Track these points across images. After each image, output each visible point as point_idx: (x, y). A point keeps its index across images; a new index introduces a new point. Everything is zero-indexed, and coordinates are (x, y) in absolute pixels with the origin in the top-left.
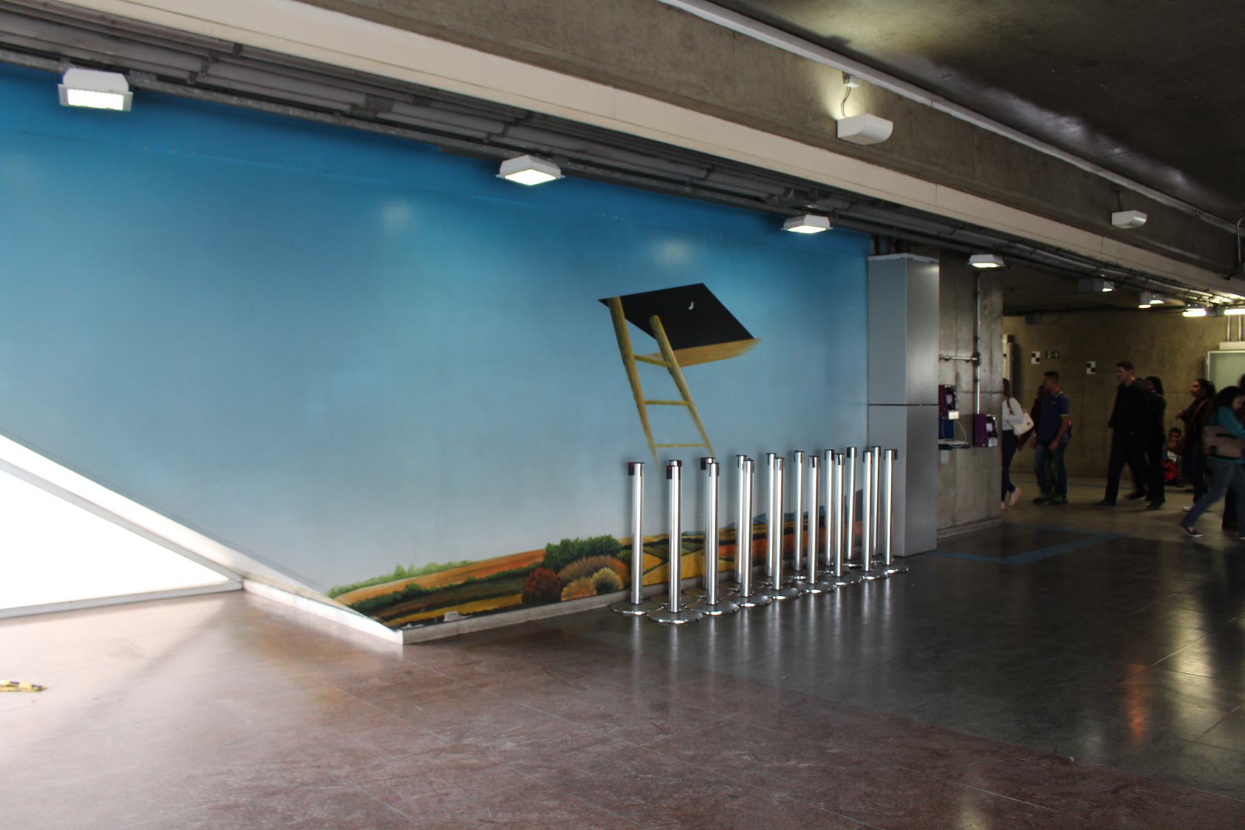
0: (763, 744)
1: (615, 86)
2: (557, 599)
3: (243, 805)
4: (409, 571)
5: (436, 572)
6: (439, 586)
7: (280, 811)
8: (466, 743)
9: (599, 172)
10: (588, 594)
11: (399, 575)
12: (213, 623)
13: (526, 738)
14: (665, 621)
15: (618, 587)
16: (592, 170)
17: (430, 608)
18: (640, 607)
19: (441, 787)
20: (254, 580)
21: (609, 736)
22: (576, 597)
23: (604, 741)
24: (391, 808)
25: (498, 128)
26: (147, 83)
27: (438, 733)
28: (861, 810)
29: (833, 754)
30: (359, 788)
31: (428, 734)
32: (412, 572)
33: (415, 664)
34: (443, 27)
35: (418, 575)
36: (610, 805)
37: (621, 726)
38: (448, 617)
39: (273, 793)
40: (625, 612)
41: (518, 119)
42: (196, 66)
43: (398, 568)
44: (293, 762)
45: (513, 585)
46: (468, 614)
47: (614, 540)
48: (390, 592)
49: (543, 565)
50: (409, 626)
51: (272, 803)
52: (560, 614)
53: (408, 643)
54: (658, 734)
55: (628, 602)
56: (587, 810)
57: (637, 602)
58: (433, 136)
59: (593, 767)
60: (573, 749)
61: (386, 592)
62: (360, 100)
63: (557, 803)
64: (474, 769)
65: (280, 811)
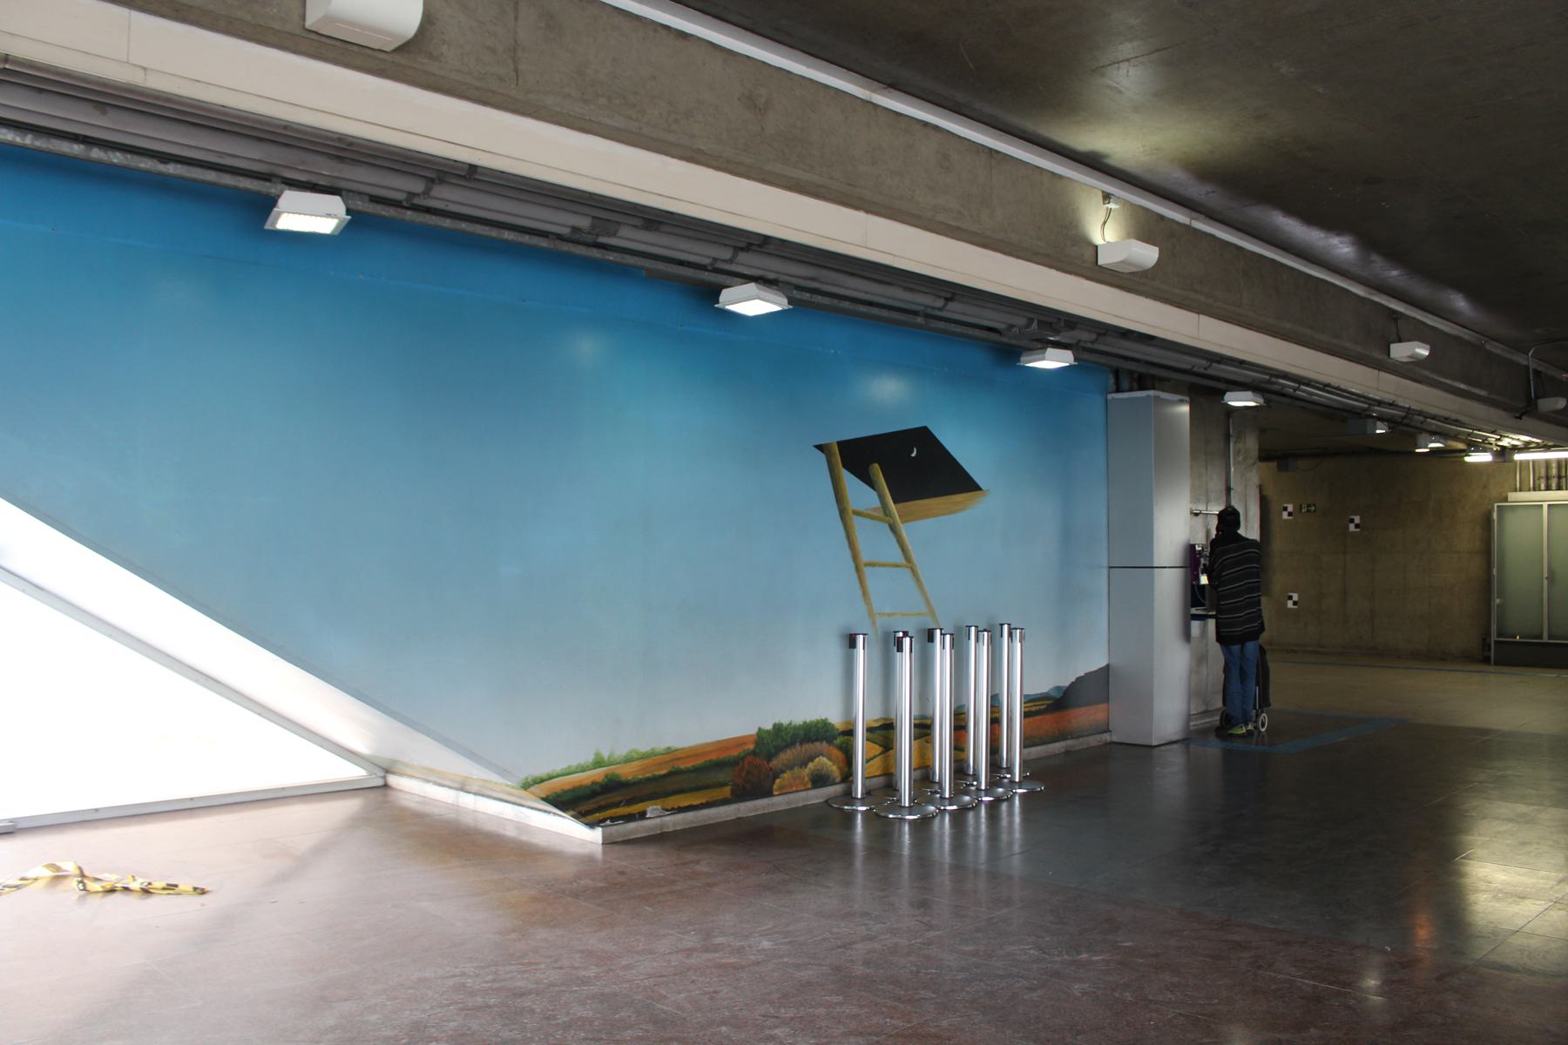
0: (1047, 939)
1: (868, 212)
2: (768, 793)
3: (495, 1006)
4: (609, 758)
5: (637, 759)
6: (641, 777)
7: (538, 1010)
8: (716, 942)
9: (826, 301)
10: (802, 788)
11: (598, 763)
12: (355, 823)
13: (782, 936)
14: (895, 816)
15: (834, 779)
16: (819, 299)
17: (630, 802)
18: (863, 801)
19: (707, 985)
20: (402, 774)
21: (874, 934)
22: (789, 790)
23: (871, 938)
24: (660, 1006)
25: (726, 254)
26: (360, 205)
27: (682, 933)
28: (1171, 999)
29: (1127, 947)
30: (616, 988)
31: (671, 935)
32: (612, 759)
33: (624, 863)
34: (700, 151)
35: (619, 763)
36: (899, 999)
37: (884, 923)
38: (651, 813)
39: (522, 995)
40: (846, 807)
41: (750, 244)
42: (417, 186)
43: (598, 754)
44: (530, 964)
45: (722, 776)
46: (673, 809)
47: (830, 724)
48: (588, 782)
49: (754, 753)
50: (608, 822)
51: (527, 1002)
52: (773, 810)
53: (608, 842)
54: (928, 930)
55: (848, 796)
56: (876, 1005)
57: (859, 796)
58: (653, 262)
59: (867, 963)
60: (840, 947)
61: (585, 783)
62: (584, 223)
63: (841, 998)
64: (735, 967)
65: (538, 1010)
